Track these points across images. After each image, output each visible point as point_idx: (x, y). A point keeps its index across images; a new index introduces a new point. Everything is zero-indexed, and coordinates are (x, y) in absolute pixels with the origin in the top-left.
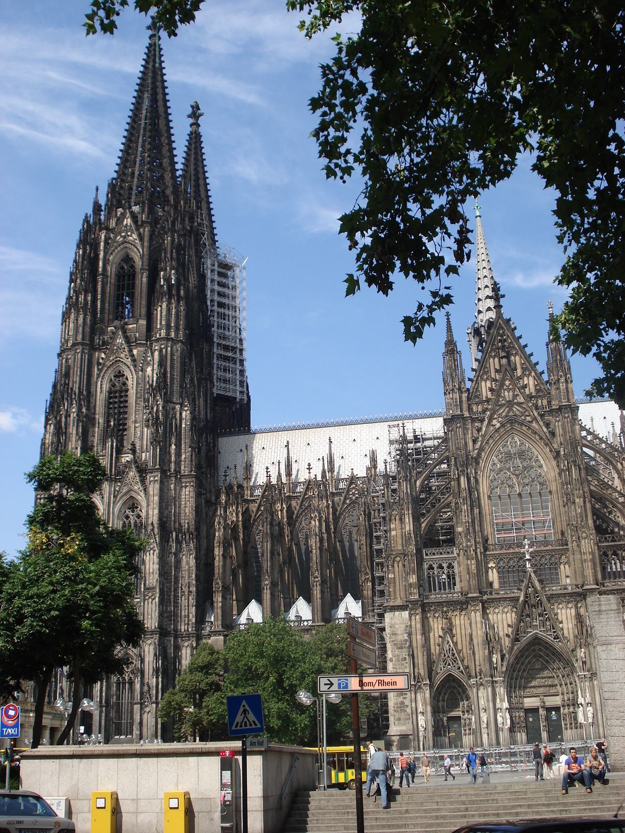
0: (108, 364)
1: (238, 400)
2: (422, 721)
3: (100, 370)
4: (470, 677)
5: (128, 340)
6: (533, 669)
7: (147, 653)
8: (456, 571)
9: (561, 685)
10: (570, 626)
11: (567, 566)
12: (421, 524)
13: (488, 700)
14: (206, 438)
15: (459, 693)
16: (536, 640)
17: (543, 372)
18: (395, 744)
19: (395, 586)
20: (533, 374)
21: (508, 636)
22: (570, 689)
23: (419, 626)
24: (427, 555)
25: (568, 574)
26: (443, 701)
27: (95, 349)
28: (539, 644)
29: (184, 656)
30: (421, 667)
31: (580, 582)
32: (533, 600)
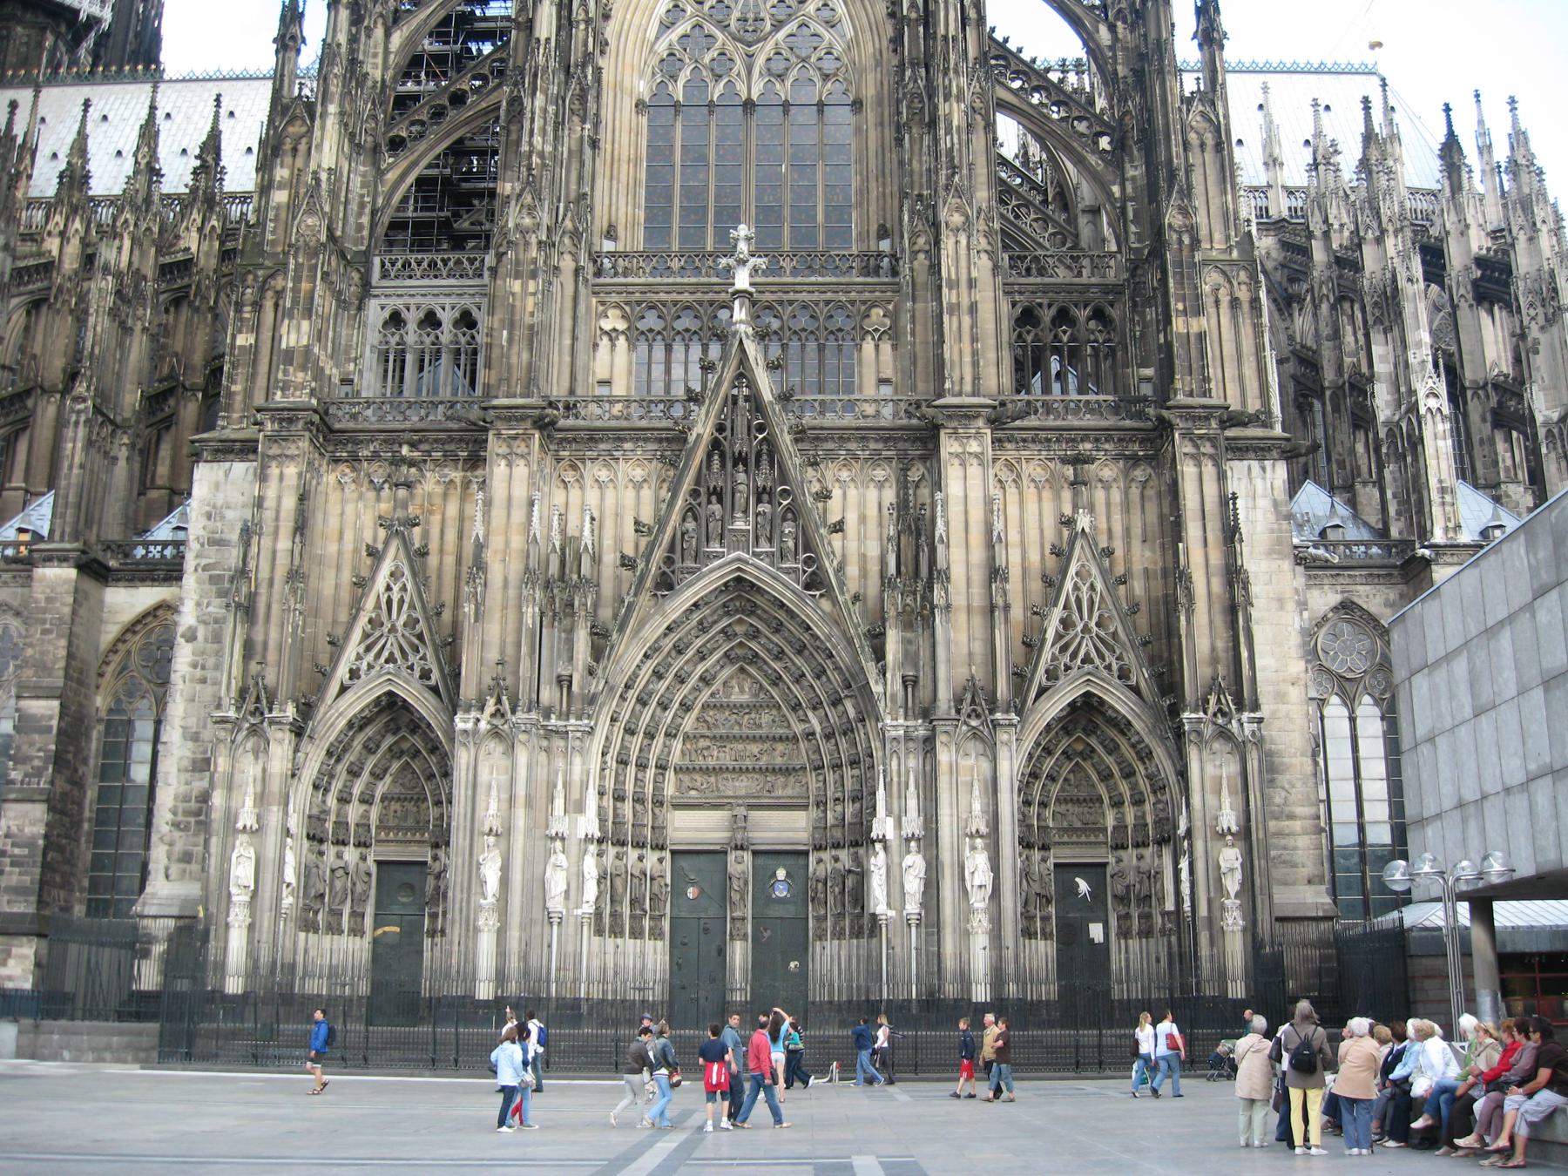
1: (83, 16)
2: (242, 871)
4: (453, 706)
6: (720, 707)
8: (481, 339)
9: (818, 768)
10: (873, 550)
11: (886, 347)
12: (380, 173)
13: (511, 800)
15: (431, 777)
16: (741, 592)
18: (158, 949)
19: (252, 377)
21: (627, 563)
22: (849, 784)
23: (290, 503)
24: (385, 275)
25: (888, 373)
26: (366, 800)
28: (753, 610)
30: (272, 656)
31: (923, 389)
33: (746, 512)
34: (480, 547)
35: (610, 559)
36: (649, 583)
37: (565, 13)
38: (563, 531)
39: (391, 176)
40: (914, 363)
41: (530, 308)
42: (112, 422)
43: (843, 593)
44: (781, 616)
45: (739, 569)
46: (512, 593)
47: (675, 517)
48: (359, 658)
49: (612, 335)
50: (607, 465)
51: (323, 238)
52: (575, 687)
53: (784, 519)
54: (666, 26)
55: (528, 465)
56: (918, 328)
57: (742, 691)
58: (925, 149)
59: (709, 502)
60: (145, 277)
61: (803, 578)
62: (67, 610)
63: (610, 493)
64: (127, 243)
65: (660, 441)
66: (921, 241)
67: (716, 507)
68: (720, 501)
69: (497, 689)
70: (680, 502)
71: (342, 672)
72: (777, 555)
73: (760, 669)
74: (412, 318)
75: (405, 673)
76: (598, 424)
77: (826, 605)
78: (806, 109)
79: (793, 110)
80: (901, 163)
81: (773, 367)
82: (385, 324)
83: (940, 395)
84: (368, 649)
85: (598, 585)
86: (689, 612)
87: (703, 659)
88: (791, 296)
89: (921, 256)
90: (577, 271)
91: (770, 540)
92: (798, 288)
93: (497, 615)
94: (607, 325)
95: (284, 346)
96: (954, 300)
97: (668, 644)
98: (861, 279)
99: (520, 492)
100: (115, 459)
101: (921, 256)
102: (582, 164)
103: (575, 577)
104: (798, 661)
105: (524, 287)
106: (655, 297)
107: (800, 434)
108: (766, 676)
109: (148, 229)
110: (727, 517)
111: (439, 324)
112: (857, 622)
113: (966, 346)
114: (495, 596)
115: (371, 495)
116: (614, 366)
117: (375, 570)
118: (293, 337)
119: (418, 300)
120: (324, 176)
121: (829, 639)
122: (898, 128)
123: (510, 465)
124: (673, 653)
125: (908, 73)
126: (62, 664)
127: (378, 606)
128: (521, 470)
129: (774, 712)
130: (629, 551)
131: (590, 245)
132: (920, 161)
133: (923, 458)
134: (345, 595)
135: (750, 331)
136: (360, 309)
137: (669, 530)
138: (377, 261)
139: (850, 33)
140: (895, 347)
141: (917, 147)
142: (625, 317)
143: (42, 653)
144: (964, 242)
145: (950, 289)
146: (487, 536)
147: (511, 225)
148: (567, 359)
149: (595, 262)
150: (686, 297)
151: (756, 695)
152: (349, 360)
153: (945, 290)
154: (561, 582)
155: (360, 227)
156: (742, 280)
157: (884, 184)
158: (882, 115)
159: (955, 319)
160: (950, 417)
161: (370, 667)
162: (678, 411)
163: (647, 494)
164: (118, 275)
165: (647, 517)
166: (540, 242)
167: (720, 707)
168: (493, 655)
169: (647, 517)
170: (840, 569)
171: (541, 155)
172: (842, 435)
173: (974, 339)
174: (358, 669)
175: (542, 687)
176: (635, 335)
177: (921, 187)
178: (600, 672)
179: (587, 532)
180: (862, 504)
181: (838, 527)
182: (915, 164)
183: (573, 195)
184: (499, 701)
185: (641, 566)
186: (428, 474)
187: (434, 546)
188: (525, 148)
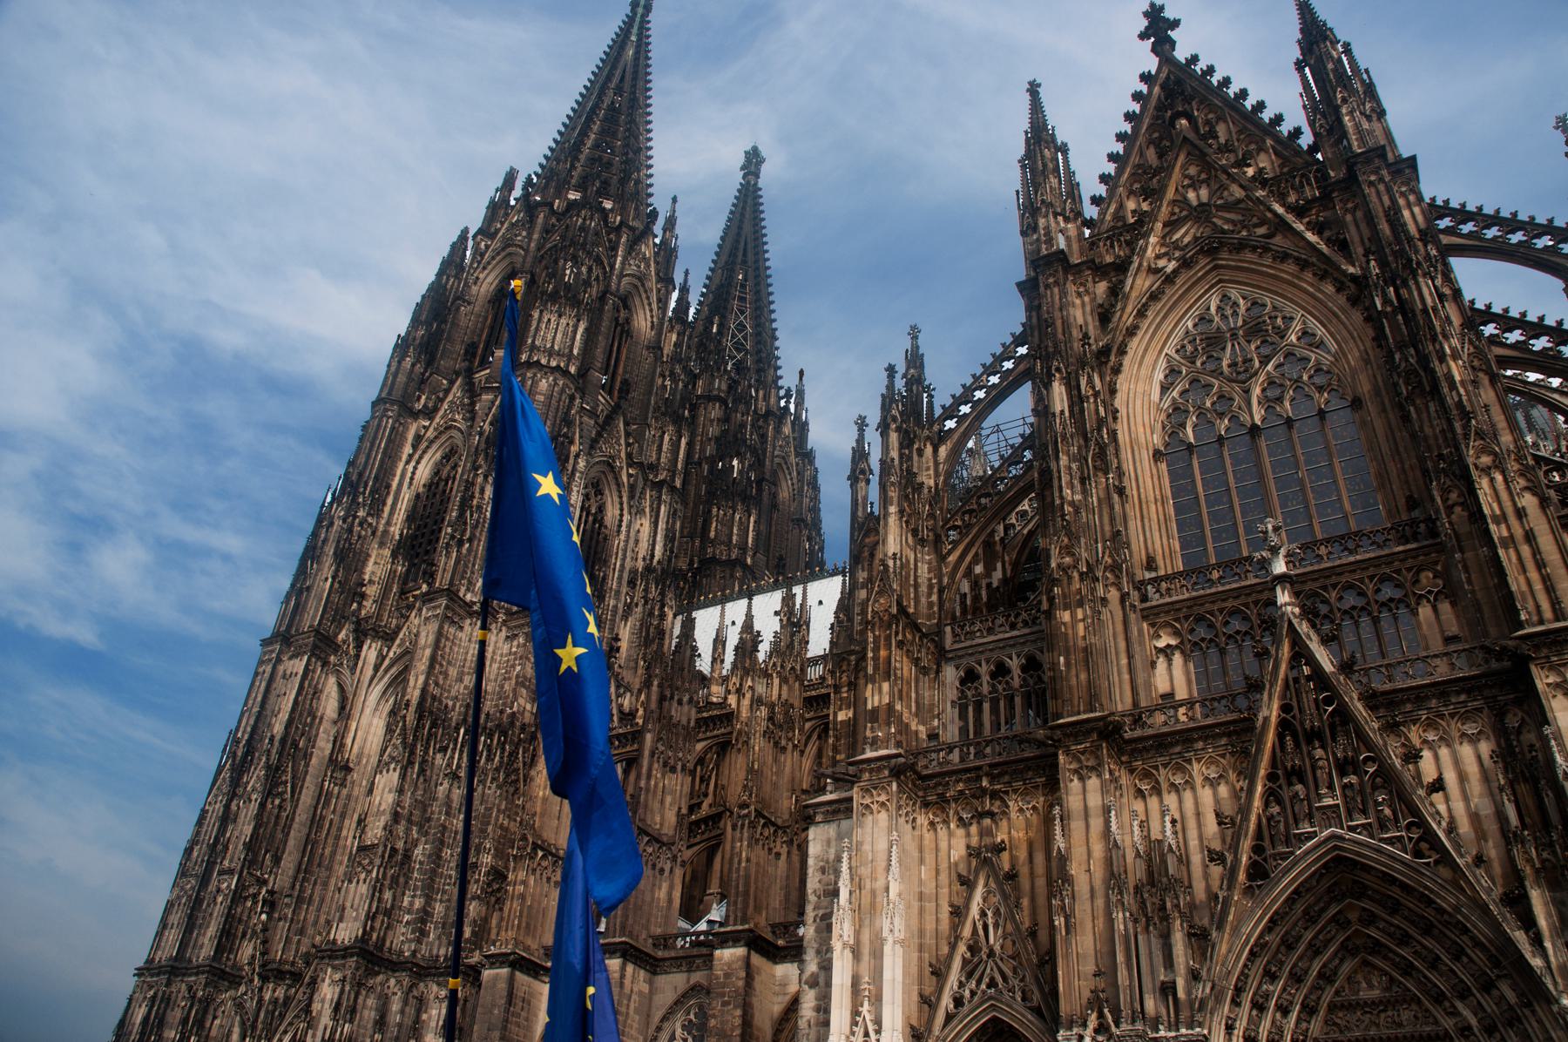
0: (430, 434)
3: (415, 447)
5: (472, 392)
6: (1350, 1007)
7: (327, 1006)
11: (1445, 607)
12: (942, 558)
14: (646, 590)
16: (1341, 872)
17: (1297, 132)
20: (1269, 142)
21: (1215, 857)
24: (955, 635)
25: (1454, 629)
27: (415, 415)
28: (1361, 891)
29: (433, 1024)
32: (1309, 708)
33: (1331, 787)
34: (1063, 859)
35: (1196, 859)
36: (1242, 876)
37: (1075, 392)
38: (1147, 838)
39: (952, 558)
40: (1479, 610)
41: (1081, 632)
42: (774, 824)
43: (1462, 856)
44: (1395, 892)
45: (1335, 847)
46: (1100, 902)
47: (1257, 803)
48: (961, 985)
49: (1167, 652)
50: (1179, 769)
51: (894, 610)
52: (1181, 994)
53: (1375, 788)
54: (1165, 389)
55: (1100, 776)
56: (1473, 576)
57: (1371, 986)
58: (1433, 414)
59: (1290, 784)
60: (792, 706)
61: (1410, 846)
62: (741, 983)
63: (1188, 796)
64: (776, 681)
65: (1229, 735)
66: (1454, 496)
67: (1299, 787)
68: (1302, 781)
69: (1096, 1003)
70: (1259, 789)
71: (946, 1002)
72: (1376, 826)
73: (1385, 958)
74: (984, 670)
75: (1007, 995)
76: (1165, 729)
77: (1445, 872)
78: (1309, 421)
79: (1297, 425)
80: (1413, 436)
81: (1325, 641)
82: (963, 682)
83: (1521, 625)
84: (970, 975)
85: (1190, 886)
86: (1290, 901)
87: (1317, 953)
88: (1334, 579)
89: (1458, 509)
90: (1124, 597)
91: (1364, 812)
92: (1338, 570)
93: (1089, 925)
94: (1161, 644)
95: (869, 707)
96: (1505, 533)
97: (1273, 939)
98: (1401, 548)
99: (1095, 800)
100: (778, 855)
101: (1458, 509)
102: (1112, 507)
103: (1164, 880)
104: (1428, 942)
105: (1073, 615)
106: (1201, 610)
107: (1373, 700)
108: (1395, 965)
109: (793, 668)
110: (1313, 795)
111: (1008, 671)
112: (1488, 886)
113: (1534, 575)
114: (1083, 910)
115: (961, 832)
116: (1173, 677)
117: (969, 899)
118: (876, 698)
119: (988, 654)
120: (891, 563)
121: (1457, 909)
122: (1401, 407)
123: (1082, 779)
124: (1283, 949)
125: (1397, 357)
126: (738, 1032)
127: (975, 931)
128: (1093, 783)
129: (1414, 1007)
130: (1216, 845)
131: (1131, 576)
132: (1432, 426)
133: (1518, 703)
134: (945, 925)
135: (1297, 610)
136: (938, 672)
137: (1253, 818)
138: (948, 629)
139: (1333, 346)
140: (1453, 604)
141: (1424, 415)
142: (1176, 633)
143: (722, 1023)
144: (1499, 477)
145: (1498, 524)
146: (1069, 848)
147: (1053, 565)
148: (1126, 677)
149: (1139, 589)
150: (1229, 604)
151: (1388, 989)
152: (933, 717)
153: (1493, 527)
154: (1153, 888)
155: (931, 605)
156: (1280, 567)
157: (1402, 462)
158: (1383, 403)
159: (1512, 552)
160: (1537, 648)
161: (973, 993)
162: (1242, 703)
163: (1223, 790)
164: (772, 706)
165: (1228, 809)
166: (1081, 574)
167: (1350, 1007)
168: (1090, 968)
169: (1228, 809)
170: (1451, 829)
171: (1072, 503)
172: (1418, 695)
173: (1540, 565)
174: (962, 997)
175: (1146, 996)
176: (1189, 648)
177: (1439, 447)
178: (1204, 973)
179: (1169, 833)
180: (1457, 762)
181: (1438, 785)
182: (1428, 430)
183: (1108, 535)
184: (1101, 1015)
185: (1229, 858)
186: (1011, 804)
187: (1024, 871)
188: (1058, 502)
